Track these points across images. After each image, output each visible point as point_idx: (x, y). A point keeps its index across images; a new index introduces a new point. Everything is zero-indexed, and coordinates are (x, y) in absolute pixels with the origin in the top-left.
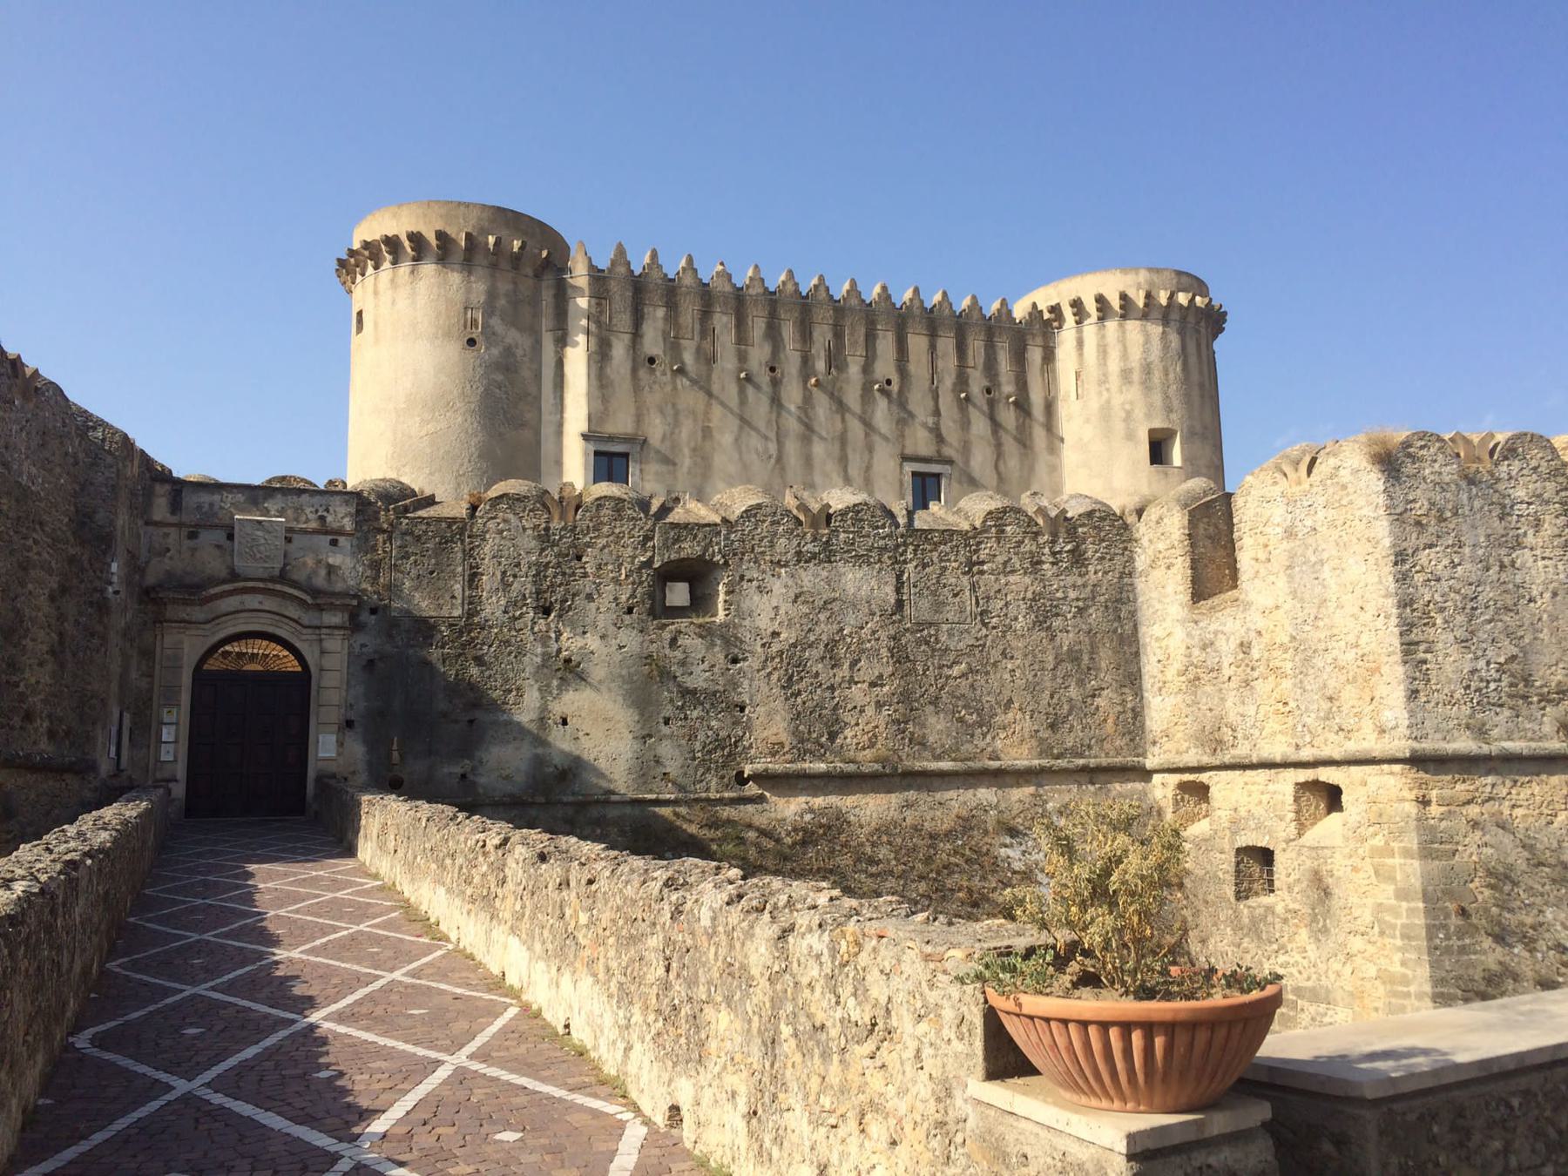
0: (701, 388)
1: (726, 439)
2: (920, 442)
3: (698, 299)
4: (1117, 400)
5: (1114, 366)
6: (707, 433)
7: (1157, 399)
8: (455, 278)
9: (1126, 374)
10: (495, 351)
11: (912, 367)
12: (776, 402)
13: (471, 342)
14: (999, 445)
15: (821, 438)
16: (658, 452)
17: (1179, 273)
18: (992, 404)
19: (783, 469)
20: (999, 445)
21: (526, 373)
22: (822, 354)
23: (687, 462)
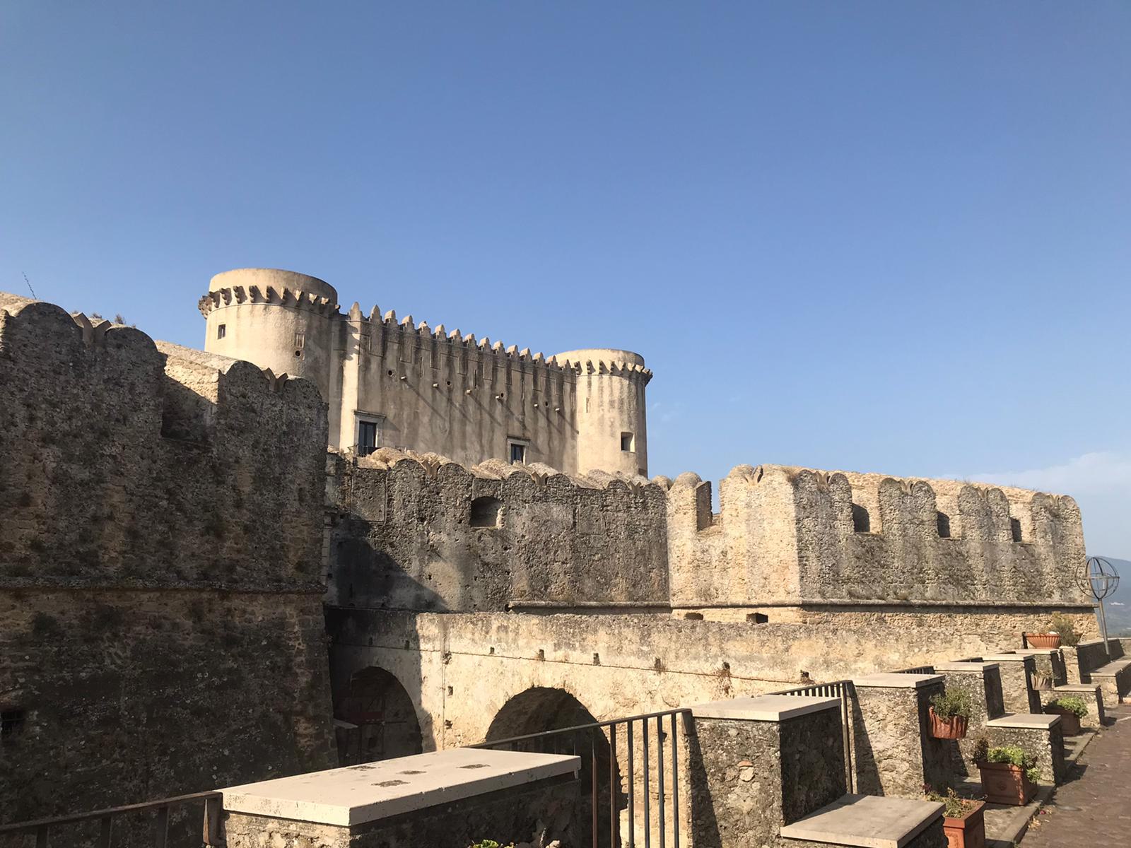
0: (414, 390)
1: (425, 419)
2: (516, 429)
3: (414, 341)
4: (607, 415)
5: (606, 398)
6: (416, 415)
7: (625, 417)
8: (291, 315)
9: (612, 403)
10: (310, 360)
11: (513, 388)
12: (450, 400)
13: (298, 353)
14: (550, 433)
15: (470, 422)
16: (392, 424)
17: (636, 355)
18: (548, 410)
19: (452, 438)
20: (550, 433)
21: (323, 373)
22: (472, 377)
23: (406, 431)
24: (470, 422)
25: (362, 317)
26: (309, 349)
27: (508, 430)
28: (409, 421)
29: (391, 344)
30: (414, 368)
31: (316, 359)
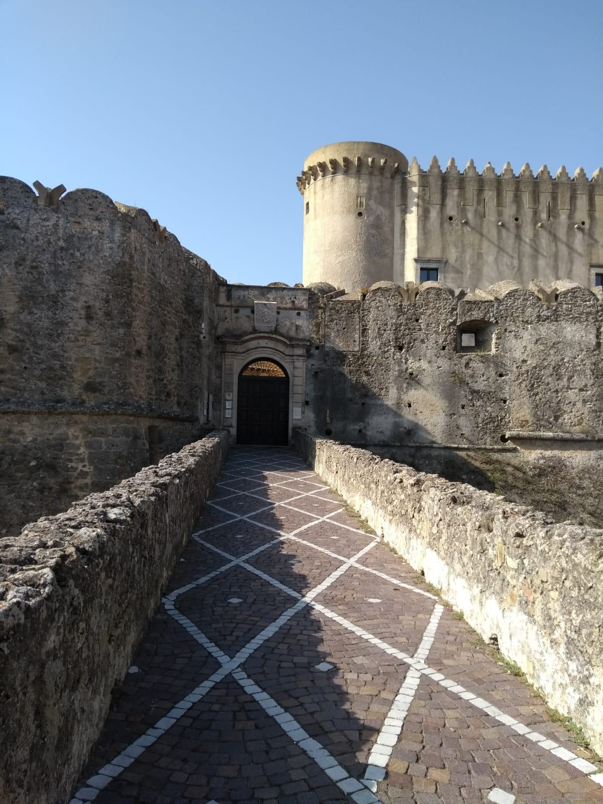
0: (477, 232)
1: (490, 259)
6: (480, 256)
8: (352, 181)
10: (372, 218)
12: (518, 237)
13: (360, 214)
15: (543, 255)
16: (453, 267)
21: (386, 229)
22: (545, 209)
23: (469, 272)
24: (543, 255)
25: (420, 171)
26: (371, 209)
27: (591, 259)
28: (472, 262)
29: (451, 190)
30: (476, 210)
31: (378, 218)
